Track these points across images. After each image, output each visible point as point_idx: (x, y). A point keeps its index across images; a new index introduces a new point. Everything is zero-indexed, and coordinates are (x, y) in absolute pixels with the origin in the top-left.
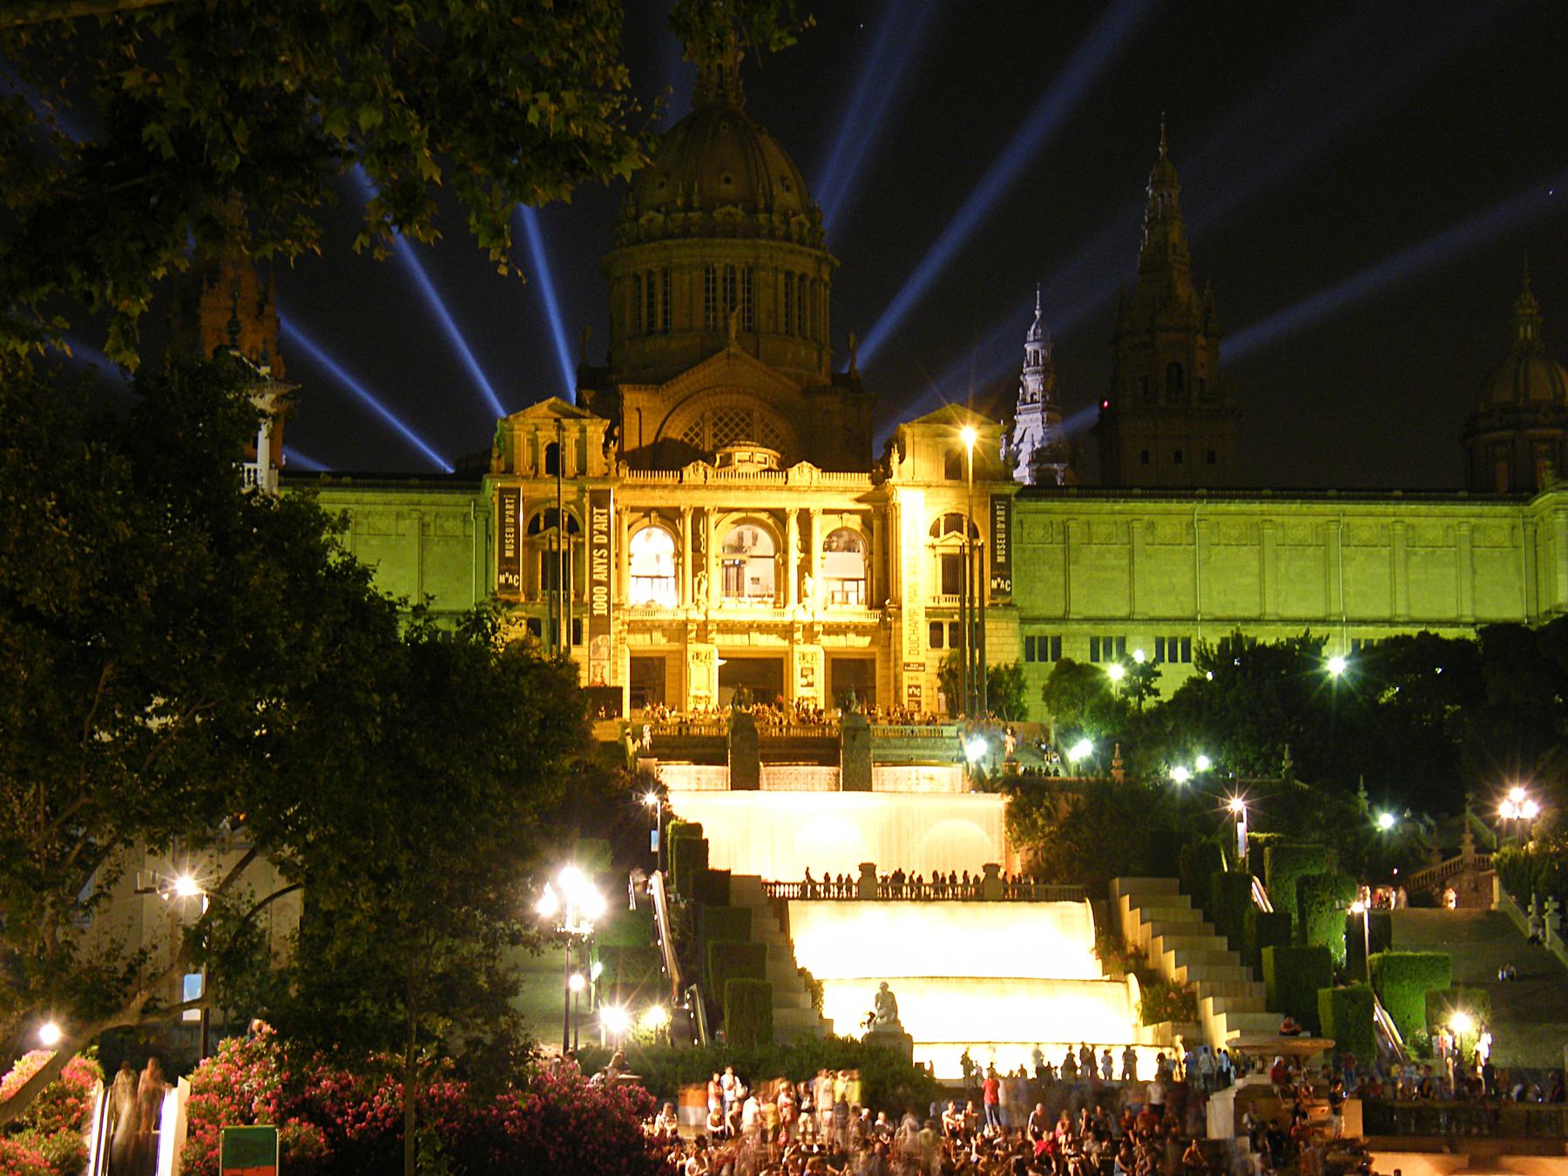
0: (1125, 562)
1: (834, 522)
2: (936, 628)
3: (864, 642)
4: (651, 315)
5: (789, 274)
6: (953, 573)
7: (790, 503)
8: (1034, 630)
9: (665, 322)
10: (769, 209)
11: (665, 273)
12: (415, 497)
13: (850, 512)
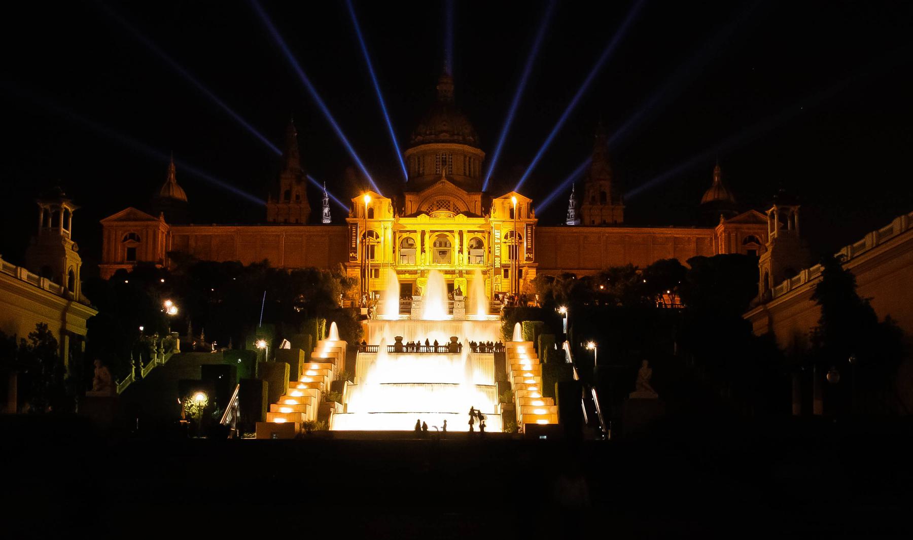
2: (506, 271)
5: (465, 157)
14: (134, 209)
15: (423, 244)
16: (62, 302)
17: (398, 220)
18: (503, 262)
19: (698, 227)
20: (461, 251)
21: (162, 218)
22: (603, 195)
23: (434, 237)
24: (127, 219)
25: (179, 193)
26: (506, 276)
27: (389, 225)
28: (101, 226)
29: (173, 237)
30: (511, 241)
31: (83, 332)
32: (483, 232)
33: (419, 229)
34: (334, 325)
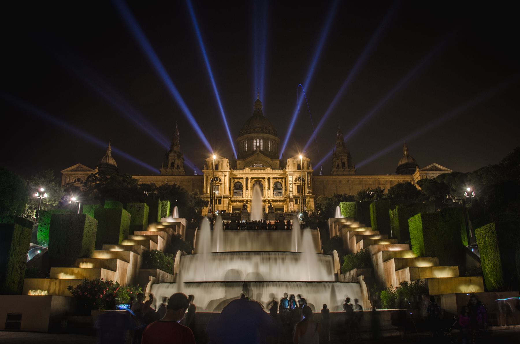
1: (276, 180)
2: (296, 200)
3: (281, 203)
6: (299, 189)
10: (266, 129)
13: (279, 178)
14: (82, 165)
17: (232, 172)
18: (294, 195)
19: (402, 175)
20: (269, 189)
22: (343, 164)
24: (76, 170)
25: (112, 161)
26: (296, 203)
27: (227, 174)
28: (62, 174)
30: (298, 183)
32: (281, 178)
33: (244, 176)
34: (176, 209)
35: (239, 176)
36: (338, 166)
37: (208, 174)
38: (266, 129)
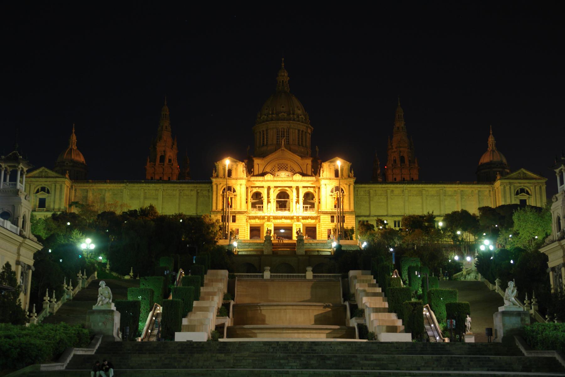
0: (385, 201)
1: (306, 190)
3: (313, 221)
4: (264, 141)
5: (299, 130)
7: (294, 185)
8: (361, 219)
9: (267, 143)
10: (293, 114)
11: (267, 130)
12: (195, 185)
13: (310, 187)
14: (46, 170)
15: (268, 197)
16: (20, 239)
20: (298, 202)
21: (67, 176)
22: (402, 159)
23: (277, 192)
29: (76, 190)
31: (31, 262)
32: (314, 187)
33: (266, 184)
35: (258, 184)
36: (395, 161)
37: (219, 184)
38: (293, 114)
